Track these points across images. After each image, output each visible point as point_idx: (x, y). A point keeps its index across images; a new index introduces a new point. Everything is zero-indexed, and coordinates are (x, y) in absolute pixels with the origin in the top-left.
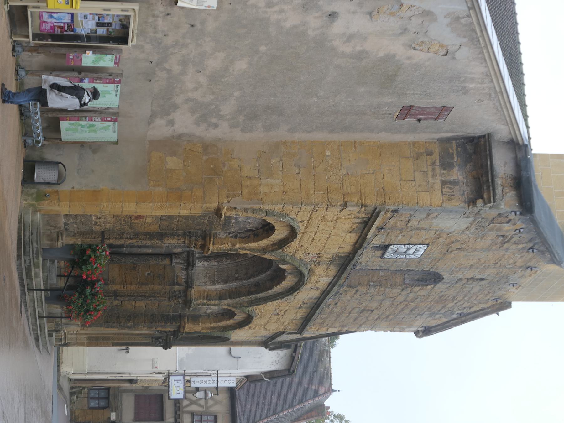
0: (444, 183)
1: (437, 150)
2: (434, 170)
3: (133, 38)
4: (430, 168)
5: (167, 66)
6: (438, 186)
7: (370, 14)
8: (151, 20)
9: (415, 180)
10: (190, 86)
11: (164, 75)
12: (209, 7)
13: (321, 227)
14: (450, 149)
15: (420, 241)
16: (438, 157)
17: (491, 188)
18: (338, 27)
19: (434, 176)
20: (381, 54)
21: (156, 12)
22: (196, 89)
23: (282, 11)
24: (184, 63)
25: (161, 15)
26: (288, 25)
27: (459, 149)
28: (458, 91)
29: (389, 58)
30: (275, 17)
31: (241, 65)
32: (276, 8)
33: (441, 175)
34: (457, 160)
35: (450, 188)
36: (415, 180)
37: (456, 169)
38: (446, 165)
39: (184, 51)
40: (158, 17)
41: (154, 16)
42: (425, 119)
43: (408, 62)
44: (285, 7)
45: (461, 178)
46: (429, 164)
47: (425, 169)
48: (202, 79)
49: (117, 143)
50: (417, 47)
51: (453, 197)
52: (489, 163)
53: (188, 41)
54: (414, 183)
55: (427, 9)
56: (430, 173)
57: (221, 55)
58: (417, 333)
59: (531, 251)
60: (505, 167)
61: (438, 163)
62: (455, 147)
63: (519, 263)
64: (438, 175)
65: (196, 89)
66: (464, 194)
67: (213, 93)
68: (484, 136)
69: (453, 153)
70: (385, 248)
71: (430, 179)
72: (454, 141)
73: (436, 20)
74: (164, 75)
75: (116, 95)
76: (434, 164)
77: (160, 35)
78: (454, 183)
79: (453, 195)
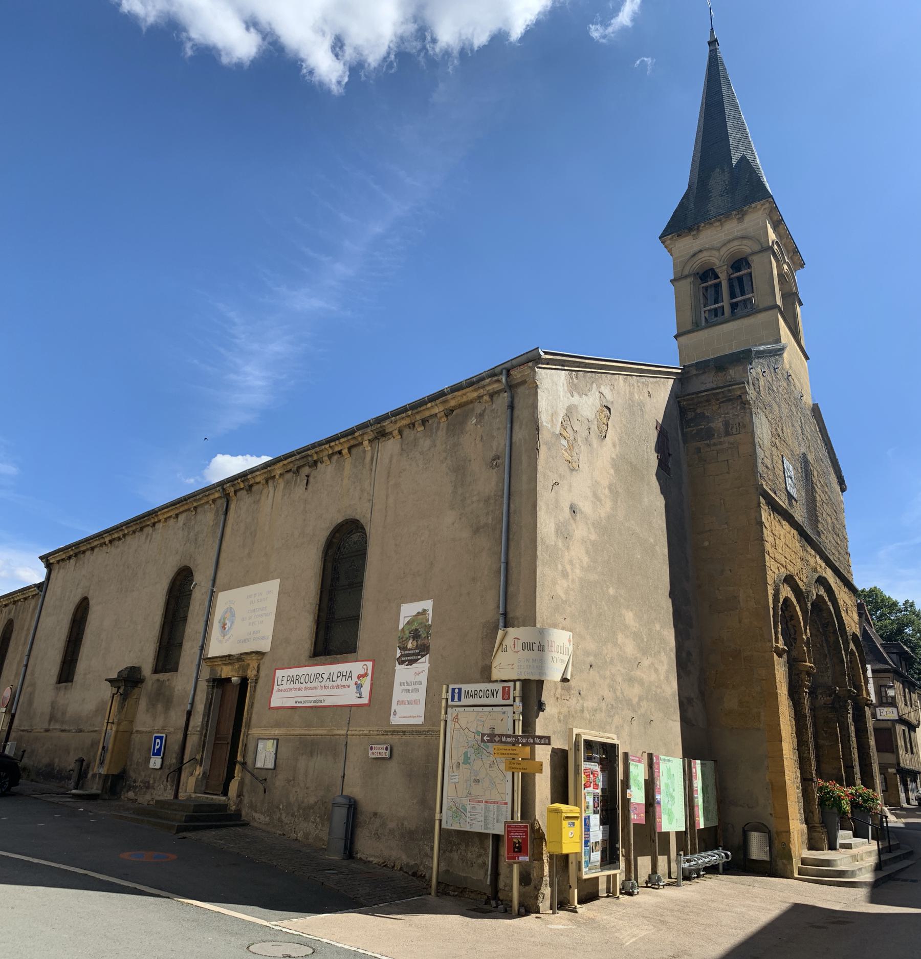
0: (727, 434)
2: (715, 445)
3: (609, 738)
4: (713, 448)
5: (635, 700)
6: (731, 439)
7: (573, 470)
8: (587, 715)
10: (653, 677)
11: (644, 704)
12: (570, 641)
13: (780, 551)
15: (780, 462)
18: (586, 507)
19: (721, 443)
20: (612, 471)
21: (578, 707)
22: (656, 670)
23: (571, 562)
24: (631, 680)
25: (581, 702)
26: (586, 560)
28: (641, 410)
30: (578, 571)
31: (629, 617)
32: (568, 568)
37: (712, 425)
38: (709, 434)
39: (619, 679)
40: (583, 706)
41: (582, 711)
42: (668, 449)
43: (618, 448)
44: (567, 557)
45: (720, 420)
46: (708, 449)
48: (646, 662)
49: (715, 761)
53: (608, 673)
56: (719, 447)
57: (620, 638)
58: (843, 490)
63: (785, 385)
65: (656, 670)
67: (659, 652)
68: (679, 402)
70: (790, 497)
73: (576, 407)
74: (644, 704)
75: (671, 761)
76: (708, 445)
77: (603, 705)
78: (726, 424)
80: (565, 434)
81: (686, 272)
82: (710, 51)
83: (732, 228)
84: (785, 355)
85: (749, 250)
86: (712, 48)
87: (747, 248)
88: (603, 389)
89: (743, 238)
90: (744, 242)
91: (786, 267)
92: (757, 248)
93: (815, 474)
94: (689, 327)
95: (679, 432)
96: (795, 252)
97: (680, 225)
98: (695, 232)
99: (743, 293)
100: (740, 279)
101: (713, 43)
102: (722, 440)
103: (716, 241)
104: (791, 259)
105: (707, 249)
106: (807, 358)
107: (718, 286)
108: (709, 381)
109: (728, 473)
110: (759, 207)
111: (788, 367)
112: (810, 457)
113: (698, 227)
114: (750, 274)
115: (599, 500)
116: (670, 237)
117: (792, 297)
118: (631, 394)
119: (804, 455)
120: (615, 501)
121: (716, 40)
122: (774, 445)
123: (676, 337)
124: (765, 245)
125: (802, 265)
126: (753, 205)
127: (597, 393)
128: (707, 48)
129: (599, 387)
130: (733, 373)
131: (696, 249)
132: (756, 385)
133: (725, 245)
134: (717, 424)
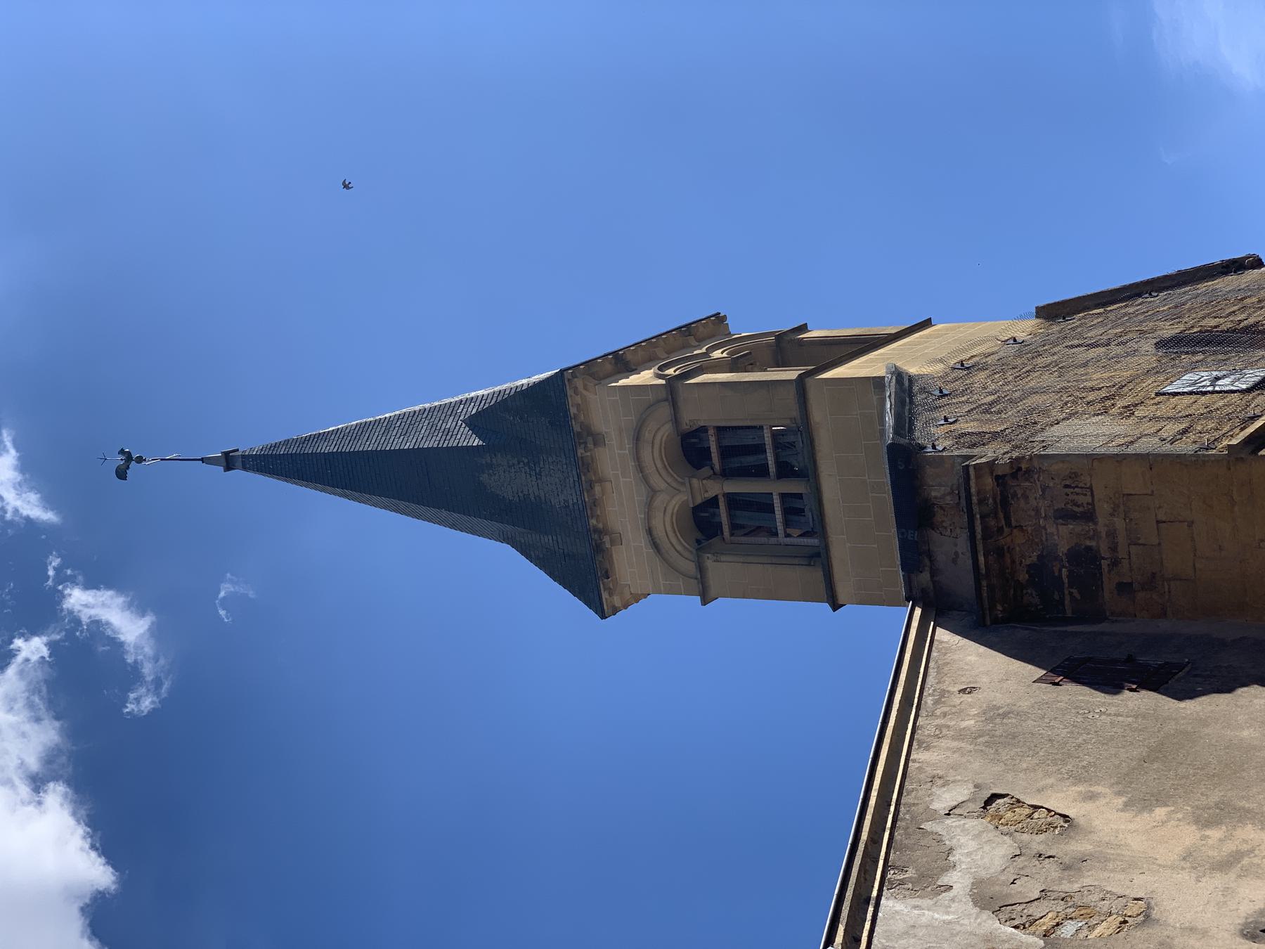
0: (1089, 516)
1: (1107, 595)
2: (1114, 549)
4: (1122, 554)
6: (1103, 509)
9: (1158, 522)
14: (1078, 597)
15: (1174, 400)
16: (1105, 579)
17: (975, 499)
20: (1161, 812)
27: (1056, 597)
28: (1005, 715)
29: (1141, 802)
33: (1096, 535)
34: (1060, 571)
35: (1076, 504)
36: (1158, 522)
37: (1063, 549)
38: (1084, 558)
45: (1051, 529)
46: (1125, 563)
47: (1133, 549)
50: (1061, 822)
51: (1068, 483)
52: (981, 559)
54: (1161, 517)
55: (987, 914)
56: (1122, 539)
59: (945, 392)
60: (956, 553)
61: (1104, 563)
62: (1067, 602)
63: (983, 375)
64: (1104, 535)
66: (1043, 491)
68: (996, 621)
69: (1071, 586)
71: (1119, 523)
72: (1069, 615)
78: (1064, 516)
79: (1067, 486)
80: (1047, 923)
81: (690, 567)
82: (245, 468)
83: (613, 462)
84: (913, 370)
85: (666, 430)
86: (239, 463)
87: (661, 432)
88: (940, 805)
89: (637, 438)
90: (647, 435)
91: (717, 354)
92: (665, 411)
93: (1213, 322)
94: (818, 574)
95: (1070, 629)
96: (688, 333)
97: (584, 572)
98: (606, 539)
99: (760, 449)
100: (726, 452)
101: (229, 461)
102: (1102, 530)
103: (633, 497)
104: (701, 341)
105: (648, 517)
106: (927, 324)
107: (735, 502)
108: (952, 546)
109: (1191, 524)
110: (578, 399)
111: (939, 367)
112: (1169, 330)
113: (596, 530)
114: (720, 430)
115: (1236, 857)
116: (605, 595)
117: (785, 346)
118: (960, 735)
119: (1162, 344)
120: (1244, 816)
121: (226, 454)
122: (1129, 411)
123: (836, 606)
124: (663, 394)
125: (719, 319)
126: (573, 410)
127: (949, 821)
128: (238, 474)
129: (933, 816)
130: (938, 488)
131: (642, 541)
132: (975, 439)
133: (645, 479)
134: (1062, 537)
